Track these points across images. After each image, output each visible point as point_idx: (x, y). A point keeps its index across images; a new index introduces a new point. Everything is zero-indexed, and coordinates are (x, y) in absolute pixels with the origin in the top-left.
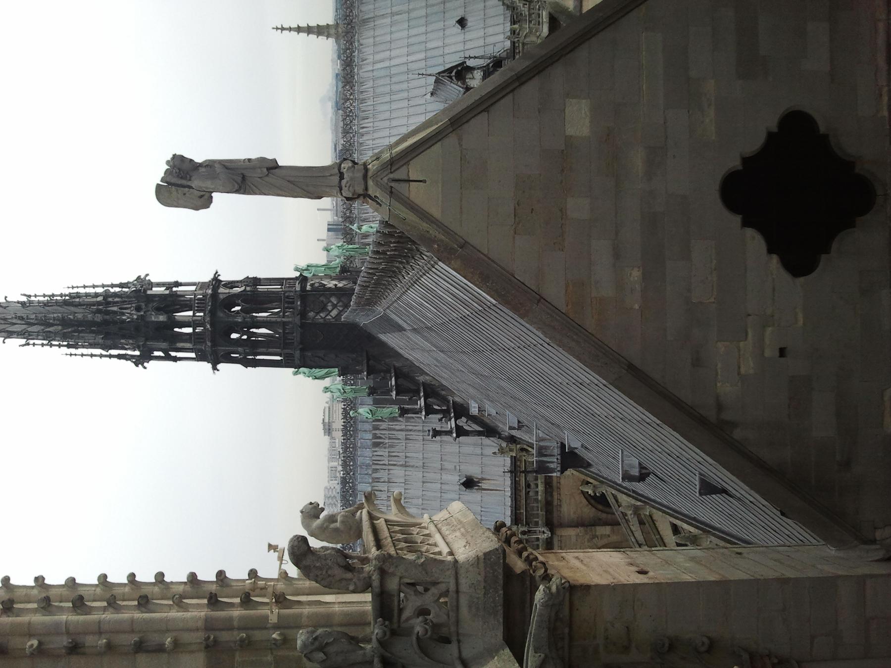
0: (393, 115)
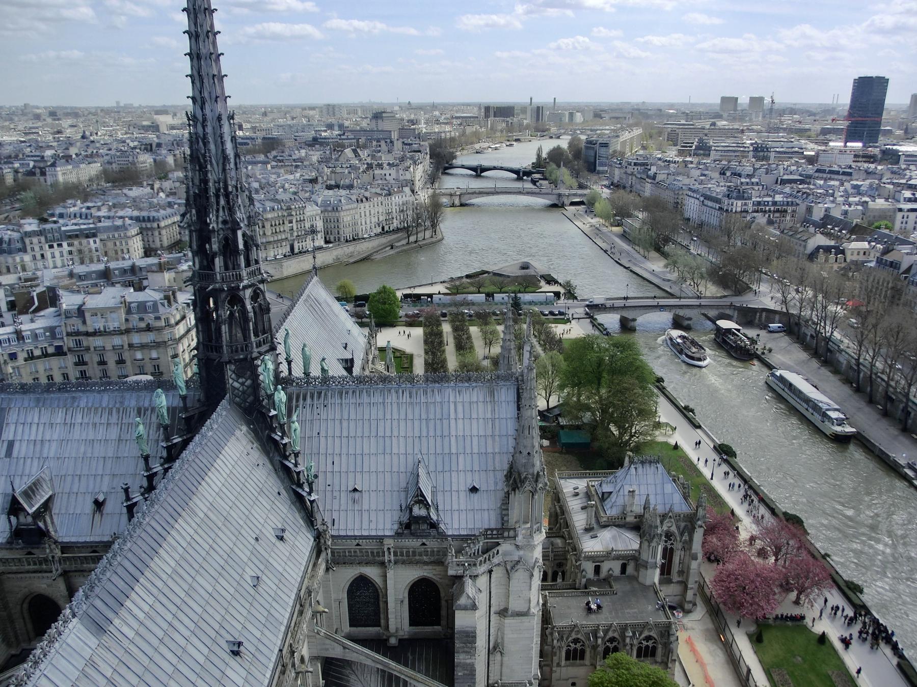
0: (409, 423)
